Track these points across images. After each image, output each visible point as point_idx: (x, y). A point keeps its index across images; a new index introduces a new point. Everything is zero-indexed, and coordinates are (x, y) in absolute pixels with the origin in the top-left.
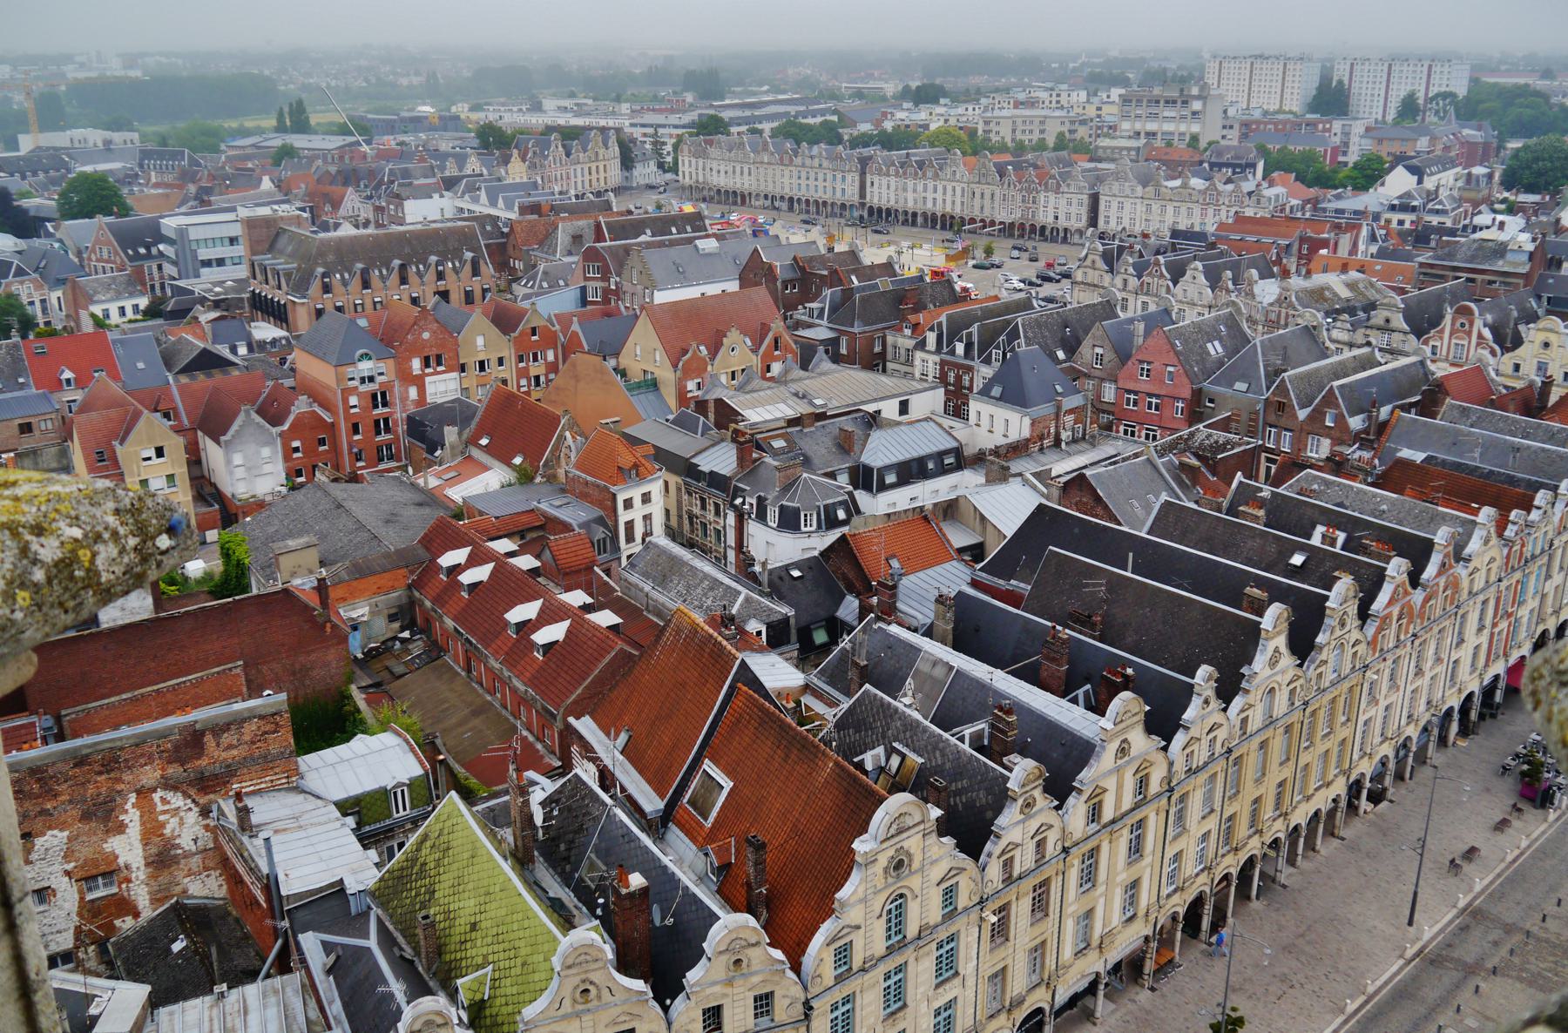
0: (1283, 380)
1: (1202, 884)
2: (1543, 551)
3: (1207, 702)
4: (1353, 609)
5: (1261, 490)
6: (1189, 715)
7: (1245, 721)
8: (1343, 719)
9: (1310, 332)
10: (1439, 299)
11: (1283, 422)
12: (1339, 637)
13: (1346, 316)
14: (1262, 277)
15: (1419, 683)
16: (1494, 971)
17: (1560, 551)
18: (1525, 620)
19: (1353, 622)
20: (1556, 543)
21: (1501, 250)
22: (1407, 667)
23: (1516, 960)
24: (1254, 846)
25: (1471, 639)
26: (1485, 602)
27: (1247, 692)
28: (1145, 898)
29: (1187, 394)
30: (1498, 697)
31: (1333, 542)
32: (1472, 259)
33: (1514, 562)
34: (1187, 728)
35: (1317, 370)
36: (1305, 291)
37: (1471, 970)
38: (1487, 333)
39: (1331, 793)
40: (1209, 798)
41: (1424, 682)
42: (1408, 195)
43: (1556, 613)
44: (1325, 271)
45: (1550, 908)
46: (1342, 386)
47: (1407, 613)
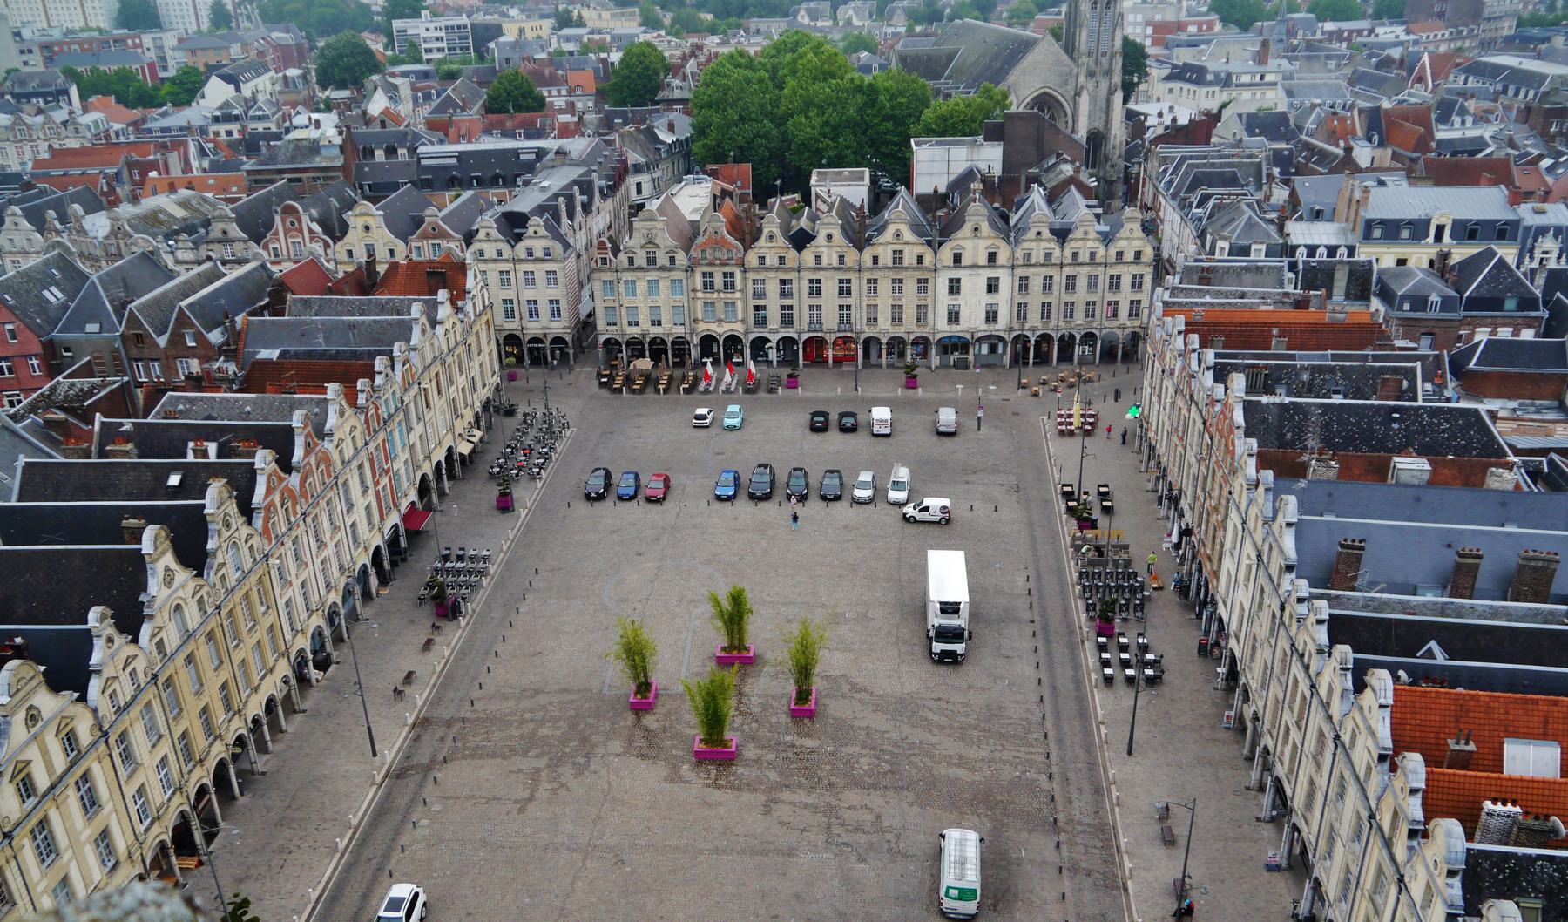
0: (131, 312)
1: (179, 804)
2: (397, 410)
3: (110, 640)
4: (232, 508)
5: (122, 425)
6: (95, 659)
7: (160, 644)
8: (263, 609)
9: (150, 258)
10: (266, 202)
11: (146, 353)
12: (230, 541)
13: (184, 236)
14: (87, 213)
15: (325, 554)
16: (445, 761)
17: (412, 406)
18: (403, 471)
19: (237, 520)
20: (406, 399)
21: (314, 147)
22: (308, 544)
23: (459, 744)
24: (219, 751)
25: (360, 502)
26: (360, 466)
27: (151, 617)
28: (121, 843)
29: (37, 349)
30: (403, 543)
31: (205, 454)
32: (292, 160)
33: (374, 424)
34: (98, 672)
35: (164, 294)
36: (138, 217)
37: (427, 769)
38: (316, 227)
39: (278, 676)
40: (151, 728)
41: (330, 550)
42: (227, 104)
43: (428, 457)
44: (155, 193)
45: (476, 693)
46: (190, 306)
47: (289, 496)
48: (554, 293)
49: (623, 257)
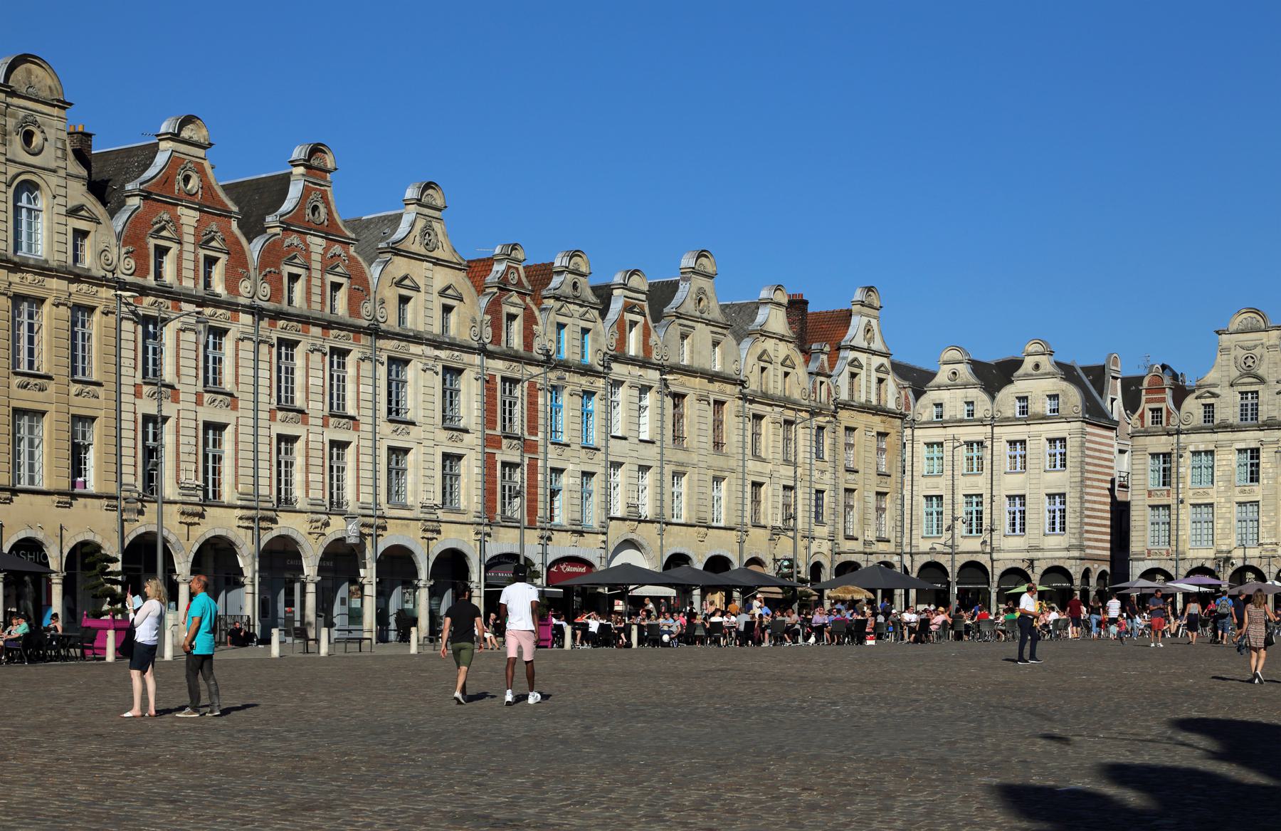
48: (1059, 480)
49: (1193, 406)
